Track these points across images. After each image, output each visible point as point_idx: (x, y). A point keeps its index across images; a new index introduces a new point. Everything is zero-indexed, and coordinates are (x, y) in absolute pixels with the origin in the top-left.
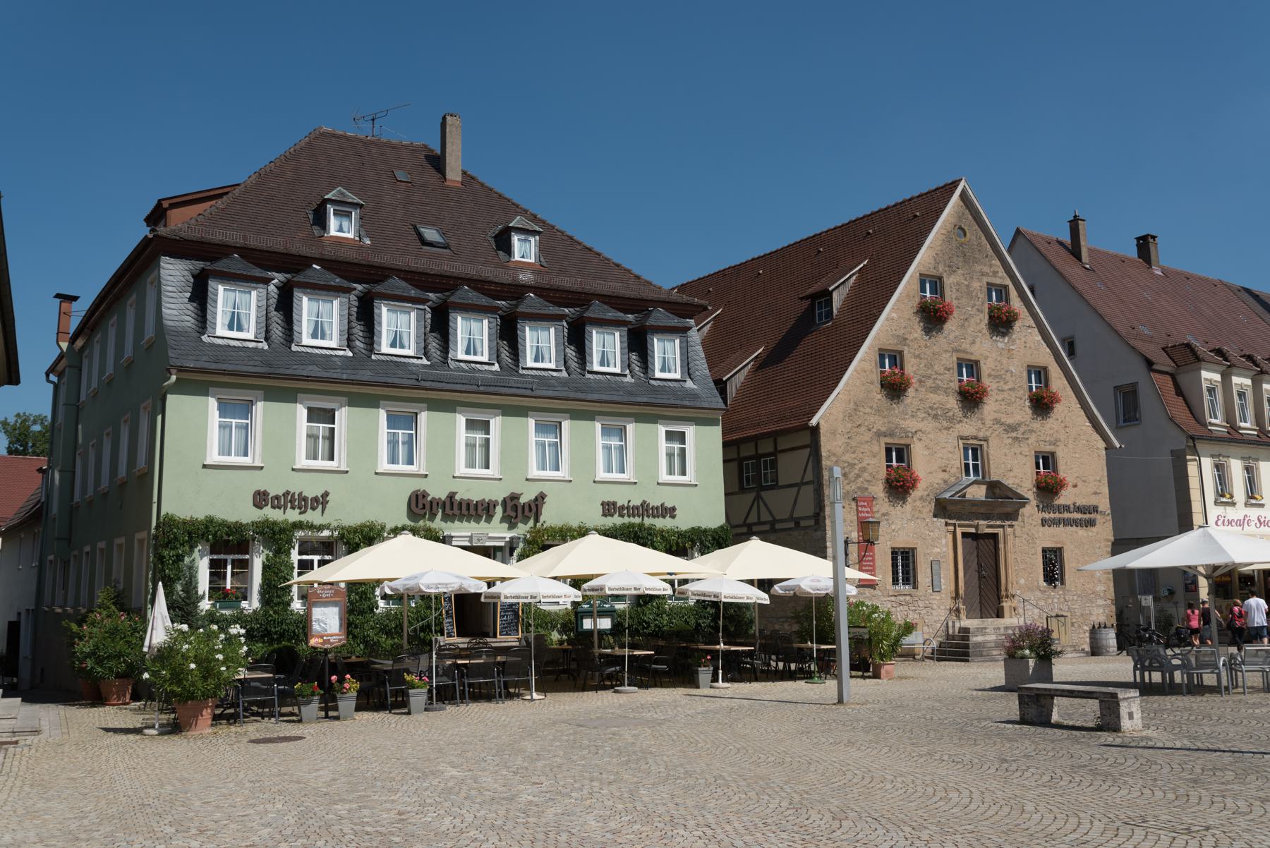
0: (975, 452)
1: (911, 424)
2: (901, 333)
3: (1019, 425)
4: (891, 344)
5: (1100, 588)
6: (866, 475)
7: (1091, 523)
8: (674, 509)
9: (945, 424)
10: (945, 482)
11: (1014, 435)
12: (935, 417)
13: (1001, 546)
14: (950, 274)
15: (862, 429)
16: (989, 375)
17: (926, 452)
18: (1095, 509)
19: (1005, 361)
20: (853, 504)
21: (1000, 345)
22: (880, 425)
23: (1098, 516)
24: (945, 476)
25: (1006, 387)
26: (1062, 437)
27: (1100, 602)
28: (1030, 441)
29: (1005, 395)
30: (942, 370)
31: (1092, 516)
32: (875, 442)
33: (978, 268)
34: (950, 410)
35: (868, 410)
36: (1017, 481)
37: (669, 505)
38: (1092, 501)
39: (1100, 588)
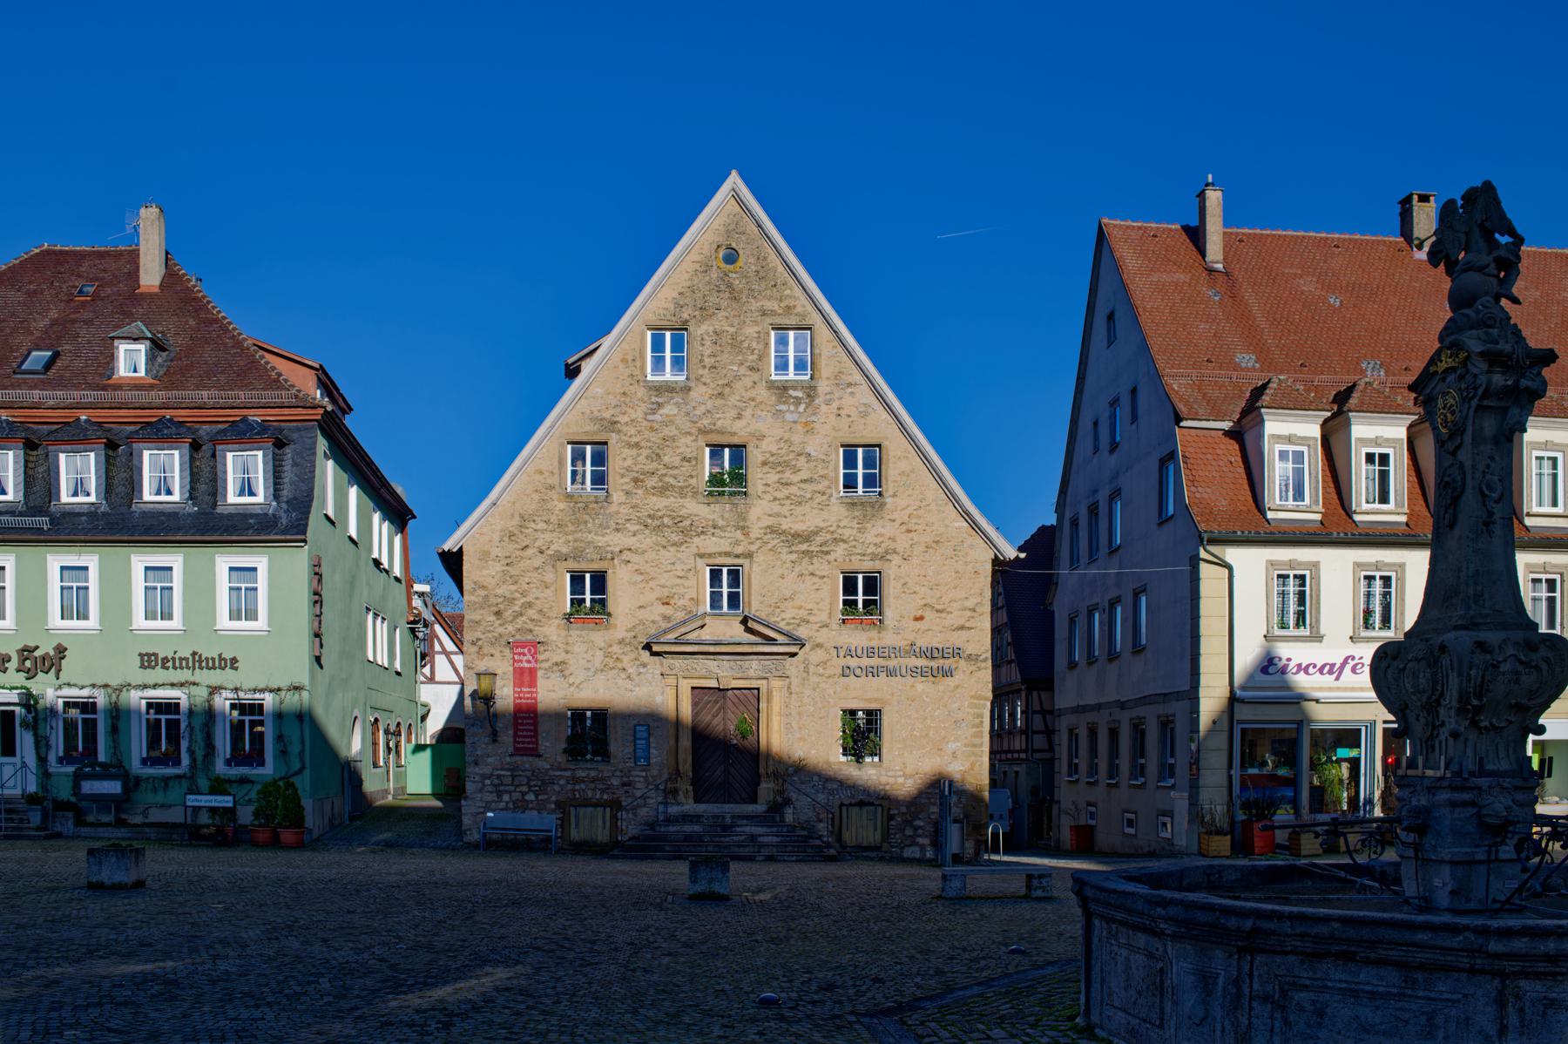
1: (615, 541)
2: (607, 415)
4: (588, 430)
6: (531, 613)
7: (948, 673)
8: (234, 660)
9: (675, 538)
10: (666, 618)
11: (804, 547)
13: (763, 705)
14: (704, 319)
15: (529, 552)
16: (764, 463)
17: (639, 578)
18: (957, 653)
19: (797, 438)
20: (507, 652)
21: (789, 417)
22: (560, 545)
25: (796, 478)
26: (902, 544)
28: (831, 557)
29: (793, 490)
30: (677, 461)
31: (947, 663)
33: (755, 305)
34: (683, 518)
35: (541, 526)
36: (802, 613)
37: (228, 655)
38: (957, 639)
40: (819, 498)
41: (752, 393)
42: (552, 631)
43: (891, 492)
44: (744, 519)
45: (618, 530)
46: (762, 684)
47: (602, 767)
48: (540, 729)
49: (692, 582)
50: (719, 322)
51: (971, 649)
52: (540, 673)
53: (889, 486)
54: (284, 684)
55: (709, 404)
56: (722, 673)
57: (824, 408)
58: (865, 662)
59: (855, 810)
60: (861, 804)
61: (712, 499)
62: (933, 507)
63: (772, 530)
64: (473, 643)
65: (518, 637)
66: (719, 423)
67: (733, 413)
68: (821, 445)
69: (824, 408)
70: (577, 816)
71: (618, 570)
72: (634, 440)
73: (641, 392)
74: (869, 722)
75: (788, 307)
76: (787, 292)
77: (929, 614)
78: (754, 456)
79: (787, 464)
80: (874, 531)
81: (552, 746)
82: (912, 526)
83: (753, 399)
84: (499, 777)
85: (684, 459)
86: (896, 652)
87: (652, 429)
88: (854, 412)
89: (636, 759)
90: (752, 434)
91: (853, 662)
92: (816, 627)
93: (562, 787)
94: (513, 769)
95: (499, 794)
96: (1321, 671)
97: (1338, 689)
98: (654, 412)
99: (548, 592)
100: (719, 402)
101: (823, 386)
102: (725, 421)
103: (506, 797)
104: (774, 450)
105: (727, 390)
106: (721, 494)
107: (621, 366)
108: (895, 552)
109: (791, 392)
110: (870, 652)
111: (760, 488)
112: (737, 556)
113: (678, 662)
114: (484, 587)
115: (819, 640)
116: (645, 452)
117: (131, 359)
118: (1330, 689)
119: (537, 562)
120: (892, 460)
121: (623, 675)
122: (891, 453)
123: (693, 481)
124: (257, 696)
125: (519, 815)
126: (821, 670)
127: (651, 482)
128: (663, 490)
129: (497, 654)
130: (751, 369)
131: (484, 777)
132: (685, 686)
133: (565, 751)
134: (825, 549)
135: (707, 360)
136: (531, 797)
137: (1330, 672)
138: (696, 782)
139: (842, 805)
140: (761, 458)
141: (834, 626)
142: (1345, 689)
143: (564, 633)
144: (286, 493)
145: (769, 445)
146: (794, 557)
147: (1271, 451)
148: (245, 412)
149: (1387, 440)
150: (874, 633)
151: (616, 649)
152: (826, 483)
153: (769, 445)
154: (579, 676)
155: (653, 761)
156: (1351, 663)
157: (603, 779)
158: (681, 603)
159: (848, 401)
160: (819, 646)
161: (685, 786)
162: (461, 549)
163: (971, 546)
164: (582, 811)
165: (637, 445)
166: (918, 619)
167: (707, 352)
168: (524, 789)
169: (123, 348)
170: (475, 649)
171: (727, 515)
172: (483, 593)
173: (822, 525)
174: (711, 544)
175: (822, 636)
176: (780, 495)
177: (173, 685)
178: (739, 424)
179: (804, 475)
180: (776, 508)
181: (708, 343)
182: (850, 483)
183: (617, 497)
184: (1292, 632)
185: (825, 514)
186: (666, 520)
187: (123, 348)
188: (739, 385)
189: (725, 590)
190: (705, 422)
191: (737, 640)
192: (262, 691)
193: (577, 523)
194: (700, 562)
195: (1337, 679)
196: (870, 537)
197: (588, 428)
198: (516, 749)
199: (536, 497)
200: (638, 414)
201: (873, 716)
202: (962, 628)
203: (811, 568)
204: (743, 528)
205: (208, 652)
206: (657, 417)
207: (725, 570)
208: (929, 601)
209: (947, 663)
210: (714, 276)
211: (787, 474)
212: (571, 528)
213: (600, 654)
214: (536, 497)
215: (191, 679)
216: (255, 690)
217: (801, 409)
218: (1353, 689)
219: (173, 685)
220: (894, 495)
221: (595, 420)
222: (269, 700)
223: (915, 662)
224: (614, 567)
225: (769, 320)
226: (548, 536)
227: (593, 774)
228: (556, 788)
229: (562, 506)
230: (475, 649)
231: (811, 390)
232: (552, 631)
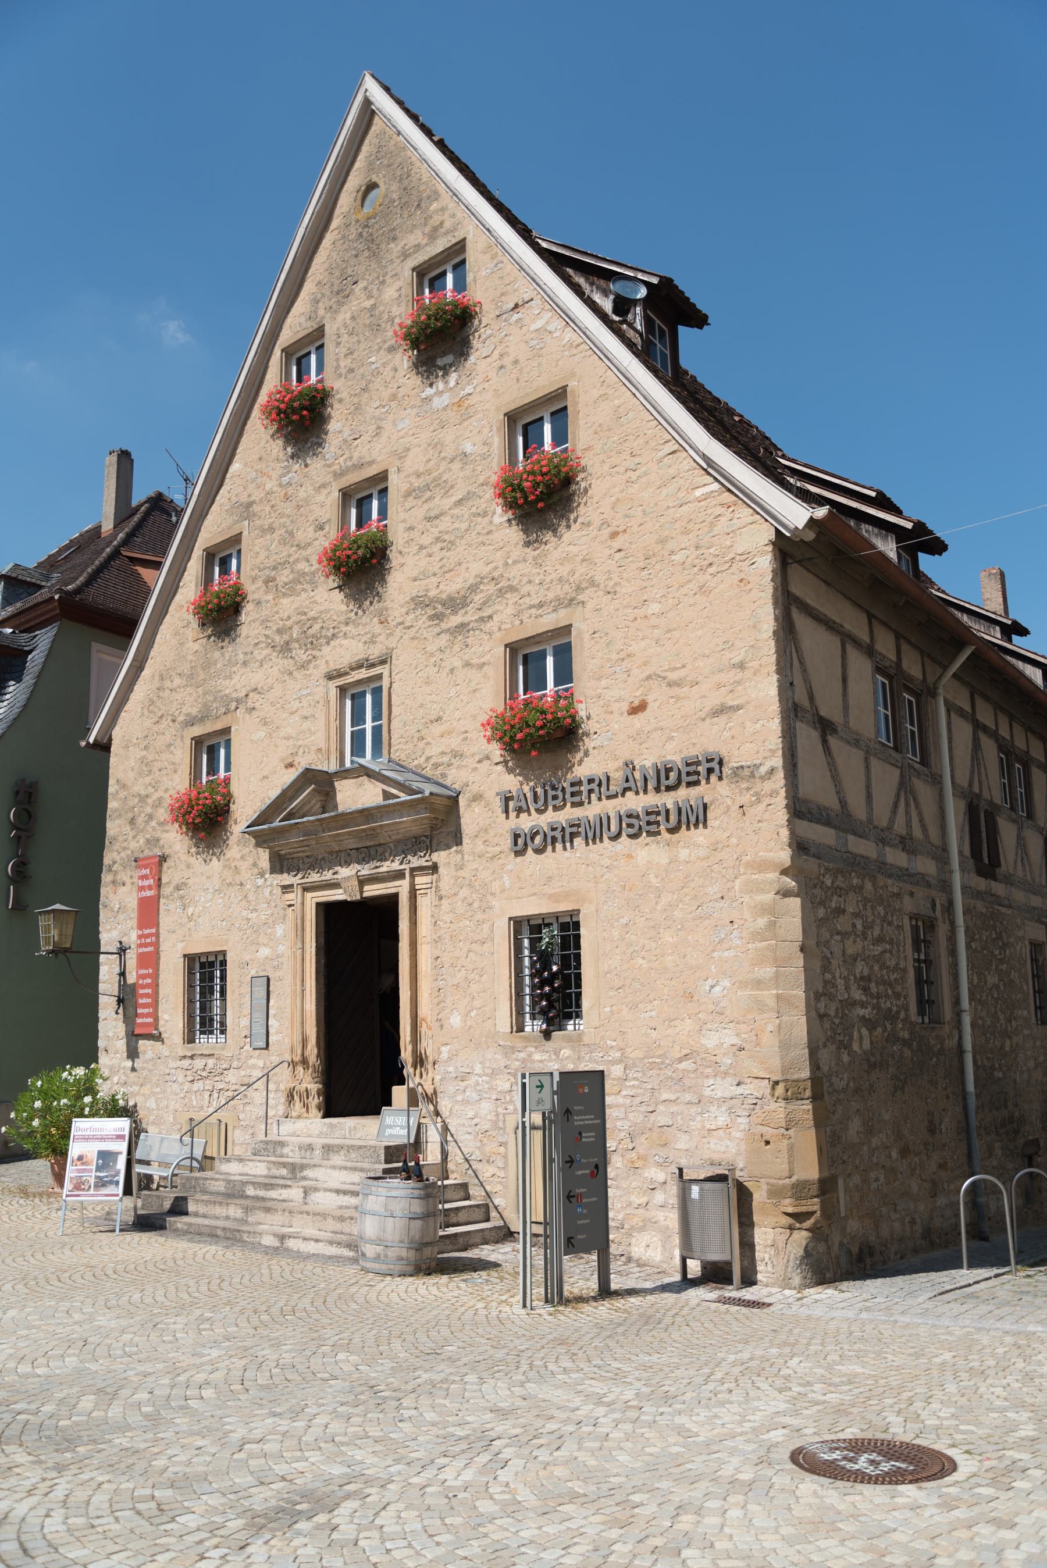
3: (473, 588)
5: (719, 1039)
7: (697, 817)
9: (301, 655)
11: (455, 620)
12: (285, 648)
15: (165, 723)
27: (724, 1088)
29: (445, 523)
33: (395, 248)
35: (177, 681)
36: (454, 742)
39: (719, 1039)
108: (592, 583)
115: (475, 789)
134: (486, 613)
140: (404, 487)
145: (415, 461)
153: (415, 461)
165: (271, 529)
166: (638, 709)
176: (426, 540)
201: (569, 929)
202: (721, 710)
223: (635, 802)
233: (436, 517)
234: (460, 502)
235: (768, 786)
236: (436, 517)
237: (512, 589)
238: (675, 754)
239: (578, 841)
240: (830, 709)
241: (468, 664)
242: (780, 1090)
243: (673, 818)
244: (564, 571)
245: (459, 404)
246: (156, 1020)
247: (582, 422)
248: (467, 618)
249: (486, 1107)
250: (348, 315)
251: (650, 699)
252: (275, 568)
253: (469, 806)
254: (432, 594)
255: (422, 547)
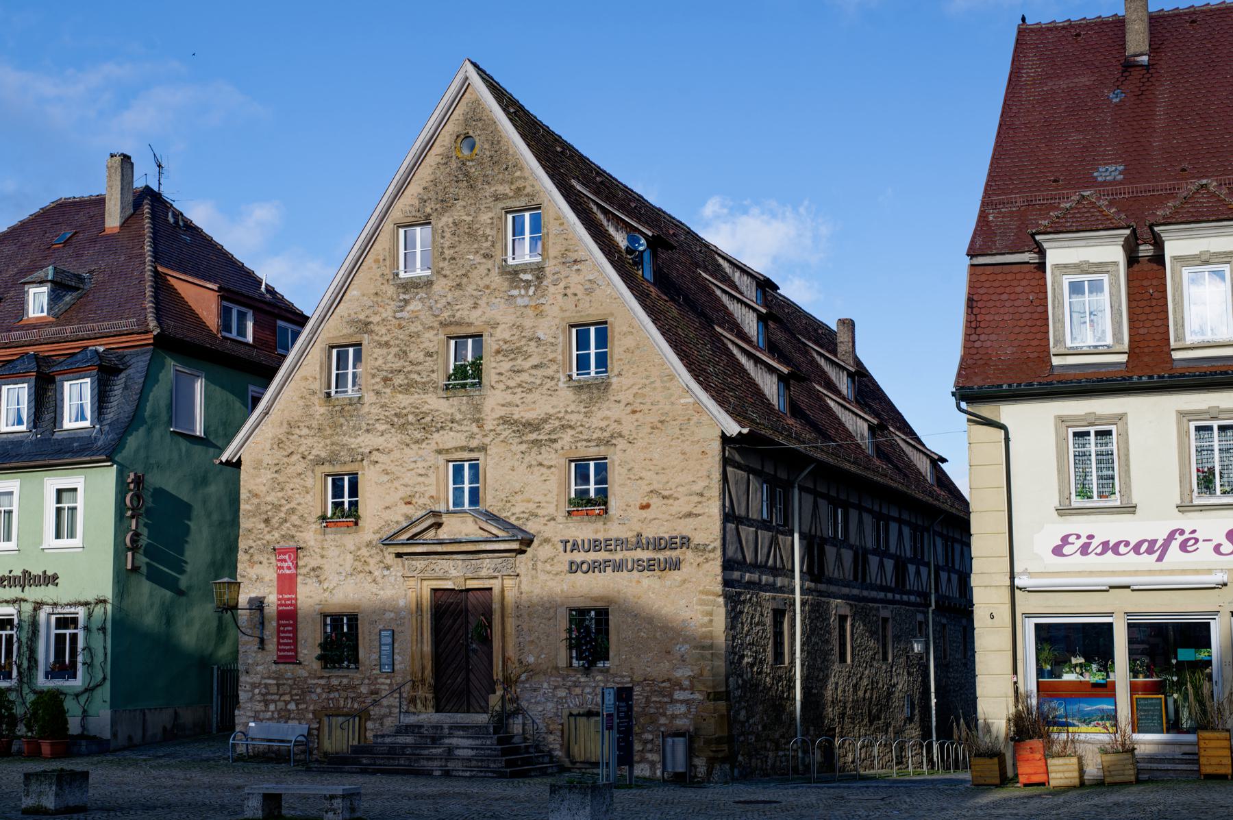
0: (467, 472)
1: (365, 442)
2: (362, 317)
3: (545, 421)
6: (294, 519)
7: (676, 565)
8: (55, 577)
9: (418, 435)
10: (407, 517)
11: (534, 436)
12: (403, 427)
14: (445, 210)
15: (294, 458)
17: (386, 478)
18: (685, 542)
19: (528, 323)
21: (520, 301)
22: (320, 451)
23: (688, 556)
24: (409, 510)
25: (527, 364)
26: (627, 427)
28: (558, 446)
29: (524, 377)
31: (674, 554)
32: (310, 473)
33: (489, 190)
35: (305, 431)
36: (532, 506)
37: (49, 573)
38: (685, 528)
40: (550, 384)
41: (486, 281)
42: (310, 536)
43: (616, 372)
44: (479, 411)
45: (368, 431)
46: (496, 585)
47: (351, 674)
48: (300, 636)
49: (432, 479)
50: (459, 212)
51: (698, 538)
52: (300, 579)
53: (614, 365)
54: (90, 597)
55: (450, 298)
56: (453, 574)
57: (552, 289)
58: (592, 556)
59: (583, 720)
60: (590, 714)
61: (450, 394)
62: (658, 384)
63: (505, 420)
64: (246, 551)
65: (282, 544)
66: (458, 315)
67: (470, 303)
68: (550, 328)
69: (552, 289)
70: (330, 726)
71: (366, 472)
72: (385, 339)
73: (390, 290)
74: (598, 622)
75: (519, 189)
76: (518, 174)
77: (655, 501)
78: (490, 344)
79: (518, 351)
80: (600, 414)
81: (309, 649)
82: (638, 407)
83: (487, 287)
84: (266, 686)
85: (429, 354)
86: (622, 543)
87: (401, 327)
88: (580, 290)
89: (381, 665)
90: (487, 323)
91: (578, 557)
92: (543, 520)
93: (319, 696)
94: (278, 676)
95: (266, 703)
96: (1136, 549)
97: (1161, 572)
98: (401, 309)
99: (309, 497)
100: (458, 293)
101: (551, 266)
102: (464, 312)
103: (272, 707)
104: (508, 338)
105: (465, 280)
106: (464, 386)
107: (375, 266)
108: (621, 436)
109: (522, 276)
110: (595, 545)
111: (494, 378)
112: (472, 450)
113: (420, 563)
114: (256, 495)
115: (546, 535)
116: (394, 350)
117: (37, 301)
118: (1150, 572)
119: (300, 467)
120: (617, 336)
121: (369, 579)
122: (617, 330)
123: (434, 376)
124: (73, 610)
125: (282, 725)
126: (548, 567)
127: (399, 380)
128: (407, 388)
129: (265, 561)
130: (486, 256)
131: (254, 686)
132: (428, 586)
133: (319, 658)
135: (447, 252)
136: (292, 706)
137: (1150, 551)
138: (437, 689)
139: (571, 714)
140: (495, 347)
141: (560, 519)
142: (1172, 572)
143: (320, 537)
144: (110, 416)
145: (502, 333)
146: (524, 447)
147: (1058, 285)
148: (85, 343)
149: (1216, 254)
150: (600, 525)
151: (364, 552)
152: (555, 367)
153: (502, 333)
154: (332, 580)
155: (397, 667)
156: (1180, 539)
157: (354, 687)
158: (421, 501)
159: (575, 279)
160: (547, 541)
161: (424, 693)
162: (239, 460)
163: (699, 423)
164: (334, 720)
165: (387, 344)
166: (645, 507)
167: (447, 244)
168: (287, 698)
169: (32, 291)
170: (247, 557)
171: (464, 408)
172: (255, 501)
173: (552, 411)
174: (449, 439)
175: (550, 531)
176: (512, 383)
177: (7, 602)
178: (478, 312)
179: (534, 361)
180: (509, 397)
181: (448, 235)
182: (583, 363)
183: (369, 397)
184: (1096, 502)
185: (554, 401)
186: (411, 418)
187: (32, 291)
188: (474, 274)
189: (467, 486)
190: (446, 314)
191: (473, 538)
192: (76, 604)
193: (335, 426)
194: (441, 459)
195: (1160, 559)
196: (595, 422)
197: (345, 331)
198: (279, 657)
199: (301, 403)
200: (387, 313)
202: (689, 515)
203: (540, 458)
204: (478, 420)
205: (36, 571)
206: (404, 314)
207: (466, 464)
208: (655, 486)
209: (674, 554)
210: (454, 166)
211: (519, 361)
212: (329, 432)
213: (349, 557)
214: (301, 403)
215: (22, 595)
216: (70, 605)
217: (531, 293)
218: (1183, 572)
219: (7, 602)
220: (620, 375)
221: (352, 322)
222: (81, 612)
223: (644, 555)
224: (363, 469)
225: (501, 205)
226: (310, 441)
227: (345, 681)
228: (314, 697)
229: (322, 410)
230: (247, 557)
231: (539, 271)
232: (310, 536)
233: (519, 372)
234: (535, 367)
235: (712, 555)
236: (519, 372)
237: (571, 427)
238: (664, 531)
239: (609, 570)
240: (740, 511)
241: (541, 464)
242: (711, 696)
243: (662, 566)
244: (603, 424)
245: (536, 307)
246: (296, 652)
247: (616, 343)
248: (540, 437)
249: (550, 706)
250: (451, 220)
251: (651, 502)
252: (392, 372)
253: (541, 544)
254: (515, 417)
255: (508, 387)
